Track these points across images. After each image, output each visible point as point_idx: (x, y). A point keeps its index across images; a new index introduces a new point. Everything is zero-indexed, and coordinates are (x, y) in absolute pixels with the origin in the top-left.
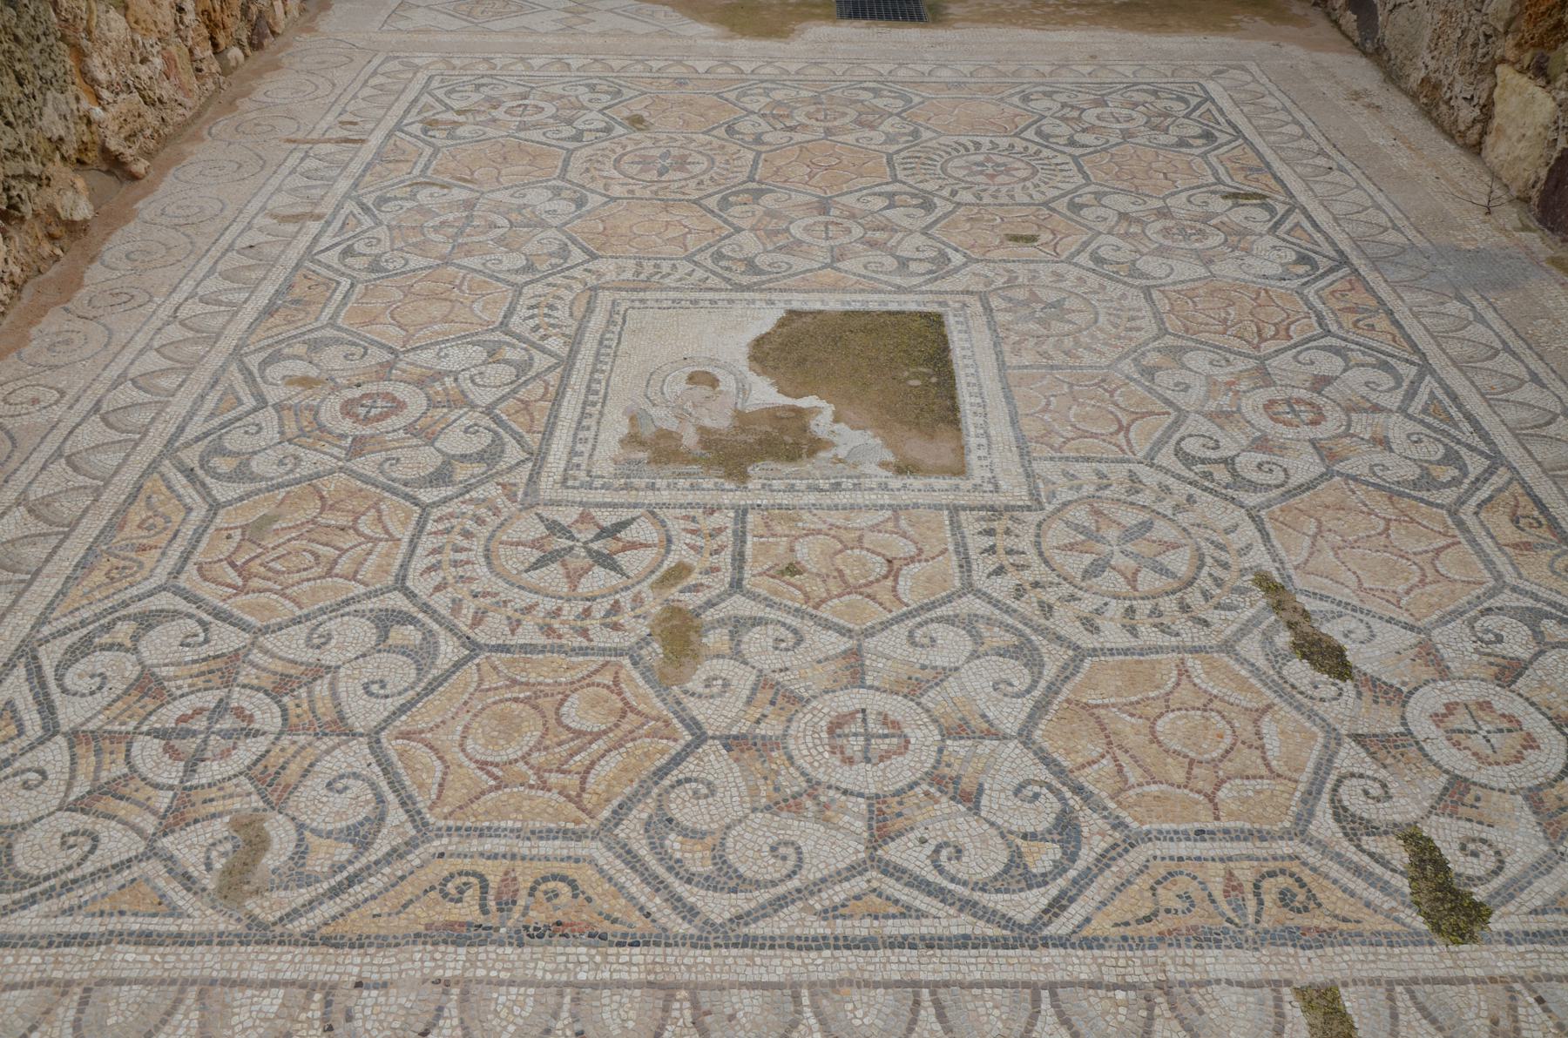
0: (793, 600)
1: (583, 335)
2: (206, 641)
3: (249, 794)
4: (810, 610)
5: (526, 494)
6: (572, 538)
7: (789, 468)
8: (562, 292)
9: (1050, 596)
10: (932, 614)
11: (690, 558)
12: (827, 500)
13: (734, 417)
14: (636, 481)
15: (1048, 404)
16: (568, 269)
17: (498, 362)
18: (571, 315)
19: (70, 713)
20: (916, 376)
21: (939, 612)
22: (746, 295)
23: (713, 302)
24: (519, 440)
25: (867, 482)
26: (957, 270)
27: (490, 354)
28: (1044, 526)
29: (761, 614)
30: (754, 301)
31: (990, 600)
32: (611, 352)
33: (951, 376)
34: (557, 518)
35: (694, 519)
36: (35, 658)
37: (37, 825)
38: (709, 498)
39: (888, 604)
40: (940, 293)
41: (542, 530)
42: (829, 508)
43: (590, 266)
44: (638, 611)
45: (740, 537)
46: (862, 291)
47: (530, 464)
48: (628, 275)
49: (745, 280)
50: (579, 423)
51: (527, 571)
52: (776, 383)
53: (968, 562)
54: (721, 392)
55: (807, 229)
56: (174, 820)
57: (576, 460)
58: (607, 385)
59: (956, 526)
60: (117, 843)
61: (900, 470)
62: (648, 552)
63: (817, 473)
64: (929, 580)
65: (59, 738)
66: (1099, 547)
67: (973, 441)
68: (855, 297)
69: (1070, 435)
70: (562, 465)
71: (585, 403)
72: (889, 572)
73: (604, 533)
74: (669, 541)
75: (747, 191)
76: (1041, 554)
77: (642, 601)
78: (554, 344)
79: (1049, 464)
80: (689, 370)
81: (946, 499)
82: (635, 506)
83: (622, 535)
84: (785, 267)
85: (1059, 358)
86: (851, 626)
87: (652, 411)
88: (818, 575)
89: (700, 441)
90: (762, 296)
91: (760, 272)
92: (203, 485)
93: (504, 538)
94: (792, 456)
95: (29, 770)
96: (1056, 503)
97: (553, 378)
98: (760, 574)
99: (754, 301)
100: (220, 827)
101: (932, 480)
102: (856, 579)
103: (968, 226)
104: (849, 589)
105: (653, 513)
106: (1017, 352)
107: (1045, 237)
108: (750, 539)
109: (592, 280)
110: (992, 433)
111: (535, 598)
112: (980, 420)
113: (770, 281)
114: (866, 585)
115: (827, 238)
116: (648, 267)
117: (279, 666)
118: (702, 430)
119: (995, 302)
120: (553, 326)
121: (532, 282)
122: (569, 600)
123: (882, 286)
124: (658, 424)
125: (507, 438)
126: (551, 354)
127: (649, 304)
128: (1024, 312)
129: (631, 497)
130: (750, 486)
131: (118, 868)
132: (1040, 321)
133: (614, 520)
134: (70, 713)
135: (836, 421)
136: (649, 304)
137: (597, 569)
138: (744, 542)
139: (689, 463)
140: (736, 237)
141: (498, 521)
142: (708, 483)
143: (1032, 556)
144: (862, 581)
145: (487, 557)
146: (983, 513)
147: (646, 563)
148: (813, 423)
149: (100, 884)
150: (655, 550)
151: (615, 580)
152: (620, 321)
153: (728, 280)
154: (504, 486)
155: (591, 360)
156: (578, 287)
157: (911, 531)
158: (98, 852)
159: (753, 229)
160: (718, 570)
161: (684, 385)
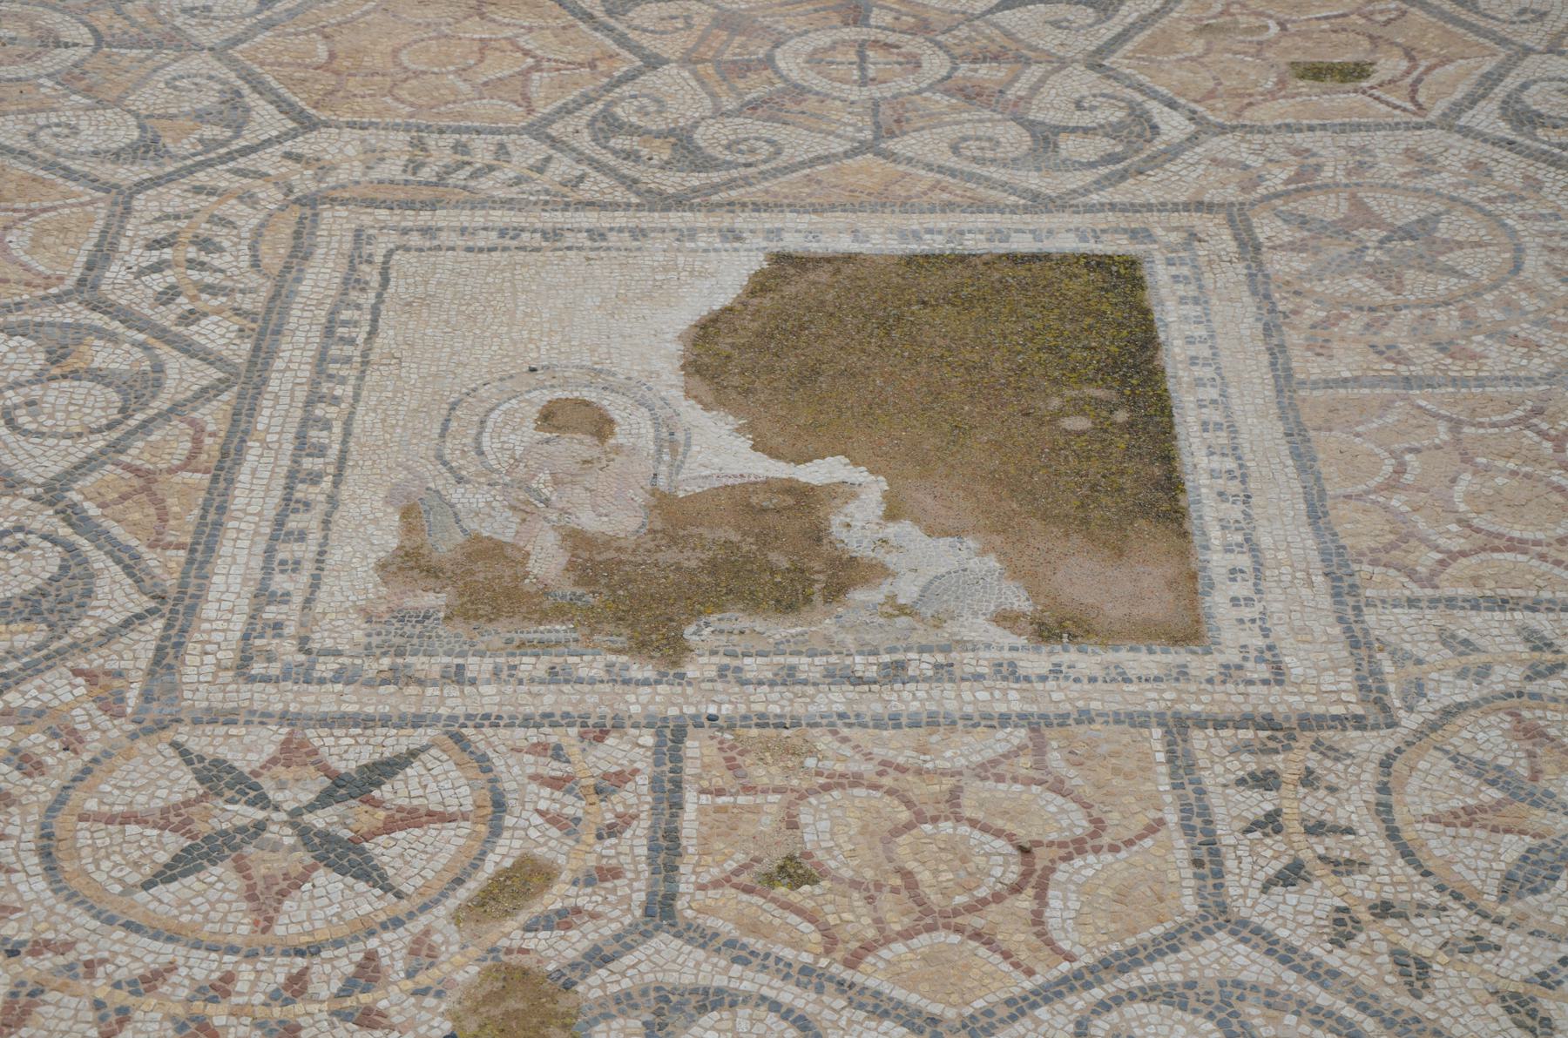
0: (797, 945)
1: (285, 312)
4: (837, 969)
5: (147, 696)
6: (261, 801)
7: (781, 629)
8: (231, 208)
9: (1421, 939)
10: (1132, 980)
11: (550, 847)
12: (872, 704)
13: (650, 509)
14: (418, 663)
15: (1401, 469)
16: (245, 151)
17: (75, 375)
18: (256, 264)
20: (1078, 406)
21: (1148, 974)
22: (675, 218)
23: (596, 234)
24: (131, 566)
25: (967, 662)
26: (1173, 152)
27: (55, 357)
28: (1397, 765)
29: (720, 981)
30: (692, 234)
31: (1272, 946)
32: (355, 353)
33: (1164, 407)
34: (224, 753)
35: (557, 753)
38: (594, 702)
39: (1023, 956)
40: (1134, 208)
41: (186, 782)
42: (879, 724)
43: (300, 145)
44: (423, 979)
45: (669, 794)
46: (947, 207)
47: (159, 624)
48: (392, 169)
49: (671, 182)
50: (280, 522)
51: (147, 885)
52: (751, 428)
53: (1215, 853)
54: (618, 449)
55: (816, 59)
57: (271, 613)
58: (347, 433)
59: (1182, 766)
61: (1047, 631)
62: (449, 830)
63: (849, 639)
64: (1121, 896)
66: (1538, 818)
67: (1217, 562)
68: (932, 221)
69: (1456, 544)
70: (239, 624)
71: (292, 476)
72: (1025, 876)
73: (340, 788)
74: (499, 805)
76: (1393, 834)
77: (433, 955)
78: (215, 333)
79: (1405, 616)
80: (543, 397)
81: (1155, 699)
82: (417, 722)
83: (384, 792)
84: (766, 150)
85: (1425, 360)
86: (936, 1009)
87: (456, 495)
88: (855, 884)
89: (571, 566)
90: (712, 220)
91: (705, 163)
93: (92, 805)
94: (789, 601)
96: (1428, 708)
97: (213, 416)
98: (716, 884)
99: (692, 234)
101: (1123, 656)
102: (945, 893)
103: (1199, 45)
104: (929, 918)
105: (458, 739)
106: (1321, 347)
107: (1390, 65)
108: (690, 797)
109: (304, 181)
110: (1265, 541)
111: (168, 952)
112: (1235, 511)
113: (730, 184)
114: (970, 909)
115: (864, 81)
116: (441, 151)
118: (576, 539)
119: (1266, 228)
120: (212, 290)
121: (155, 182)
122: (252, 955)
123: (995, 195)
124: (472, 525)
125: (99, 560)
126: (208, 357)
127: (445, 238)
128: (1338, 249)
130: (691, 671)
132: (1377, 272)
133: (367, 756)
135: (891, 515)
136: (445, 238)
137: (322, 876)
138: (677, 806)
139: (544, 617)
140: (649, 79)
141: (75, 764)
142: (591, 666)
143: (1372, 839)
144: (961, 899)
145: (46, 854)
146: (1246, 734)
147: (442, 860)
148: (836, 521)
150: (466, 827)
151: (368, 902)
152: (375, 280)
153: (631, 183)
154: (91, 677)
155: (306, 373)
156: (270, 197)
157: (1074, 778)
159: (688, 60)
160: (616, 873)
161: (529, 433)
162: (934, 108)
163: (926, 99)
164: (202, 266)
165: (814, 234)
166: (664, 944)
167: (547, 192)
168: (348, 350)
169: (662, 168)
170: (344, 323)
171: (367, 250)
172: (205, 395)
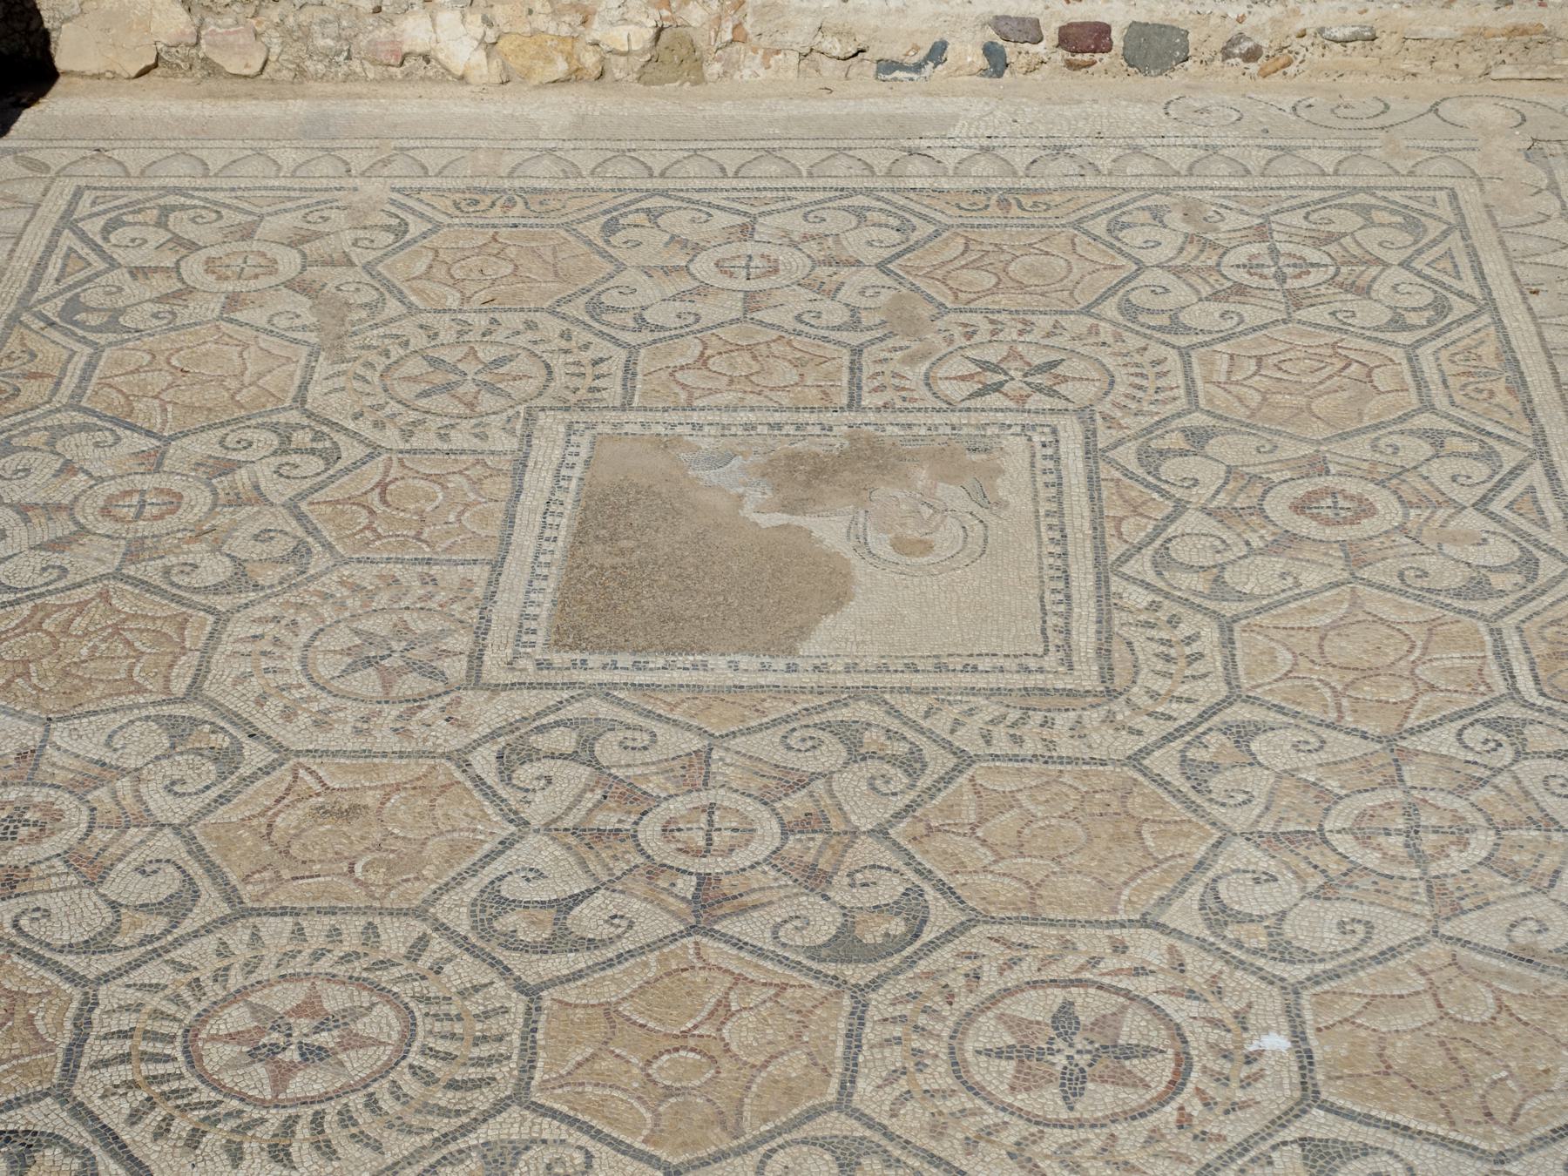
11: (906, 370)
35: (904, 399)
38: (888, 417)
42: (760, 408)
45: (855, 385)
48: (1063, 721)
49: (863, 711)
75: (874, 954)
90: (833, 680)
97: (1115, 549)
113: (820, 709)
128: (419, 653)
129: (974, 418)
136: (1010, 664)
152: (1049, 632)
162: (661, 779)
163: (666, 789)
164: (1162, 642)
165: (764, 668)
166: (855, 343)
167: (950, 703)
168: (1053, 585)
169: (869, 724)
170: (1060, 602)
171: (1061, 654)
172: (1124, 558)
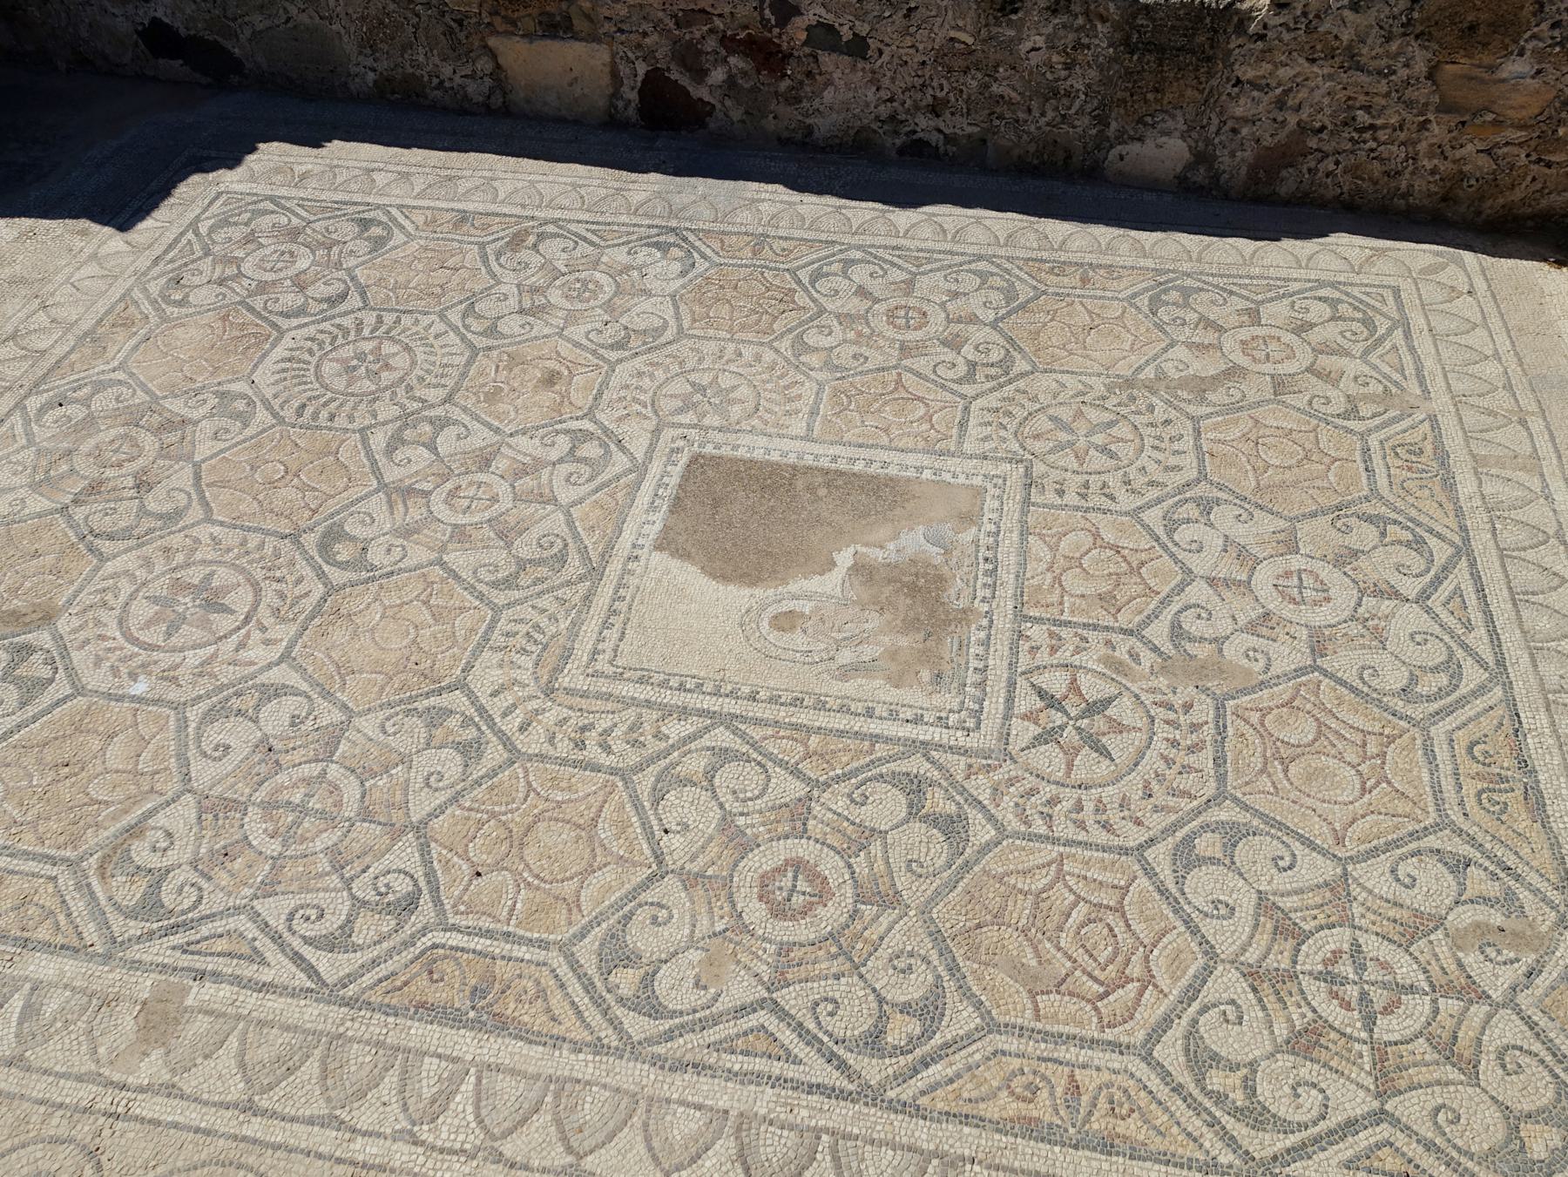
2: (1233, 1002)
3: (1431, 942)
19: (1353, 1101)
36: (1275, 1158)
37: (1500, 1098)
56: (1471, 992)
60: (1507, 1029)
65: (1387, 1107)
92: (947, 1045)
95: (1436, 1123)
100: (1471, 959)
117: (1263, 939)
131: (1532, 1025)
134: (1353, 1101)
149: (1552, 1035)
158: (1519, 1043)
